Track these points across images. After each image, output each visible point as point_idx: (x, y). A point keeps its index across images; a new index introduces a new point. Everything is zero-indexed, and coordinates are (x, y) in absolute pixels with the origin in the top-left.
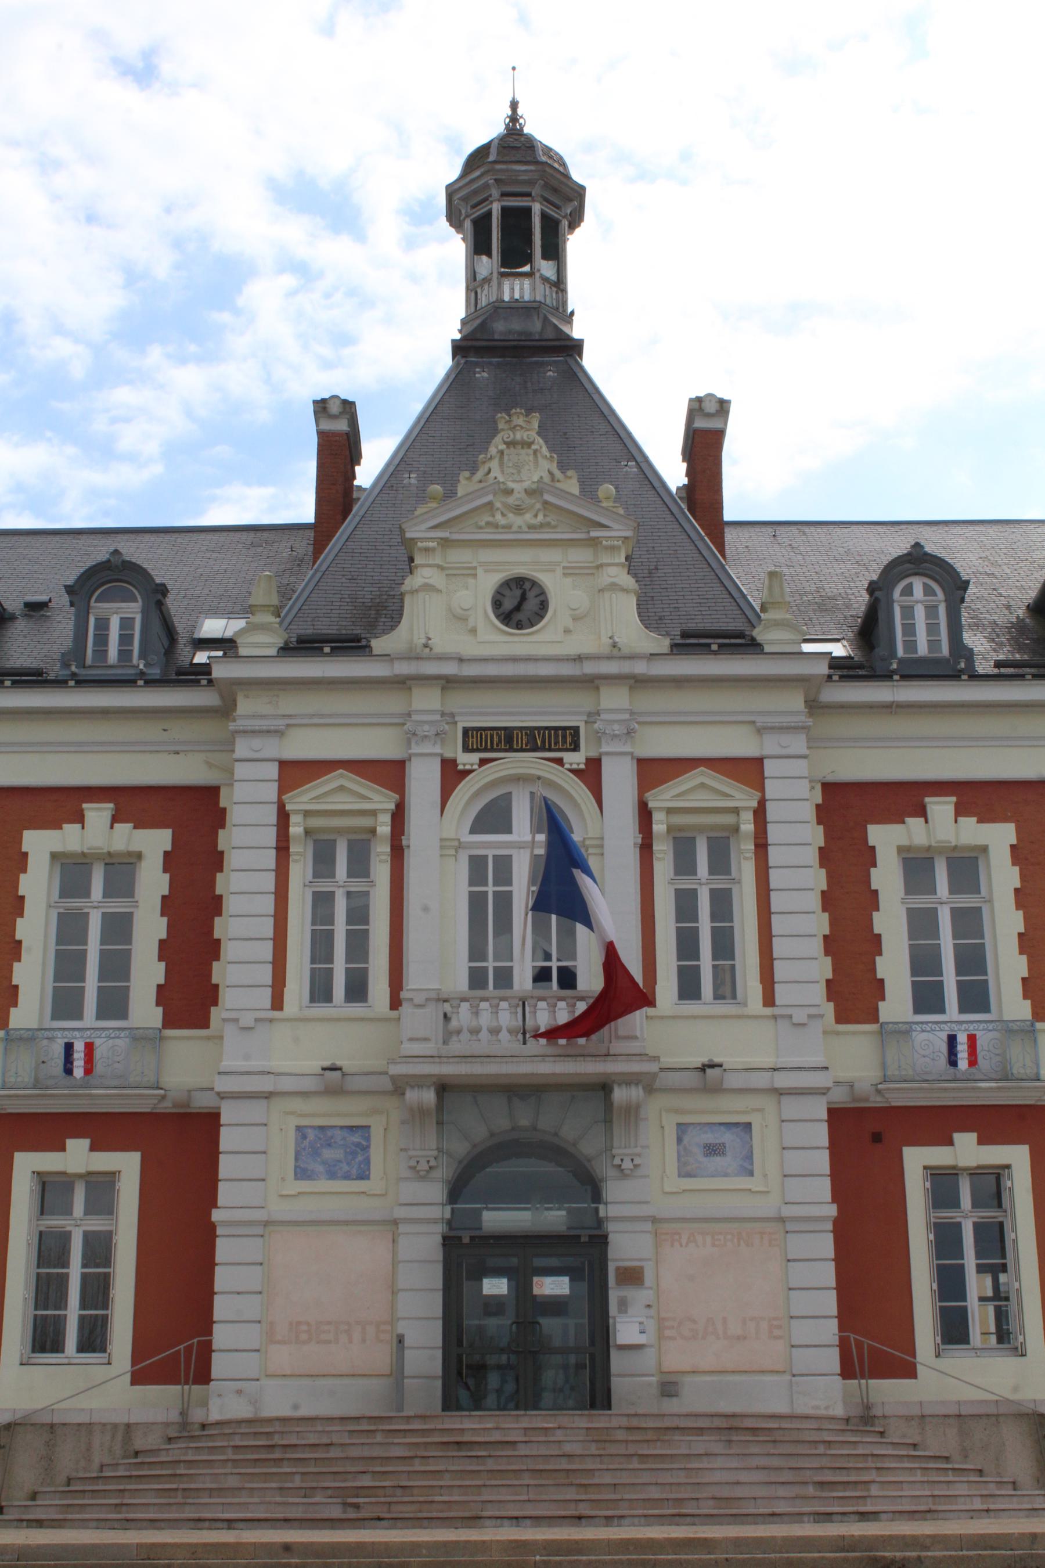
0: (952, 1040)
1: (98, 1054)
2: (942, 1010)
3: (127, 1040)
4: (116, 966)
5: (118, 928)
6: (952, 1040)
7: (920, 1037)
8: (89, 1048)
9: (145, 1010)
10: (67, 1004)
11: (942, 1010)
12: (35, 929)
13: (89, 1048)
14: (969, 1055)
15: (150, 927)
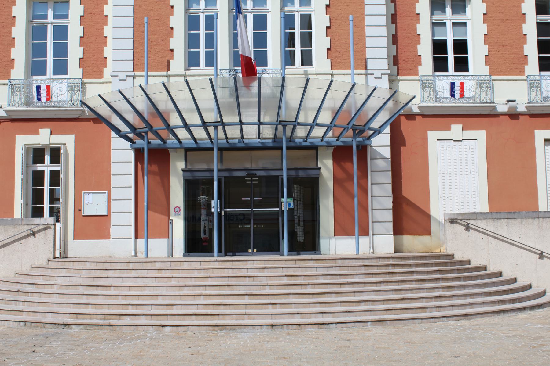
0: (453, 84)
1: (53, 90)
2: (447, 70)
3: (66, 84)
4: (61, 50)
5: (62, 32)
6: (453, 84)
7: (438, 83)
8: (48, 88)
9: (75, 70)
10: (37, 68)
11: (447, 70)
12: (19, 32)
13: (48, 88)
14: (460, 92)
15: (75, 31)
